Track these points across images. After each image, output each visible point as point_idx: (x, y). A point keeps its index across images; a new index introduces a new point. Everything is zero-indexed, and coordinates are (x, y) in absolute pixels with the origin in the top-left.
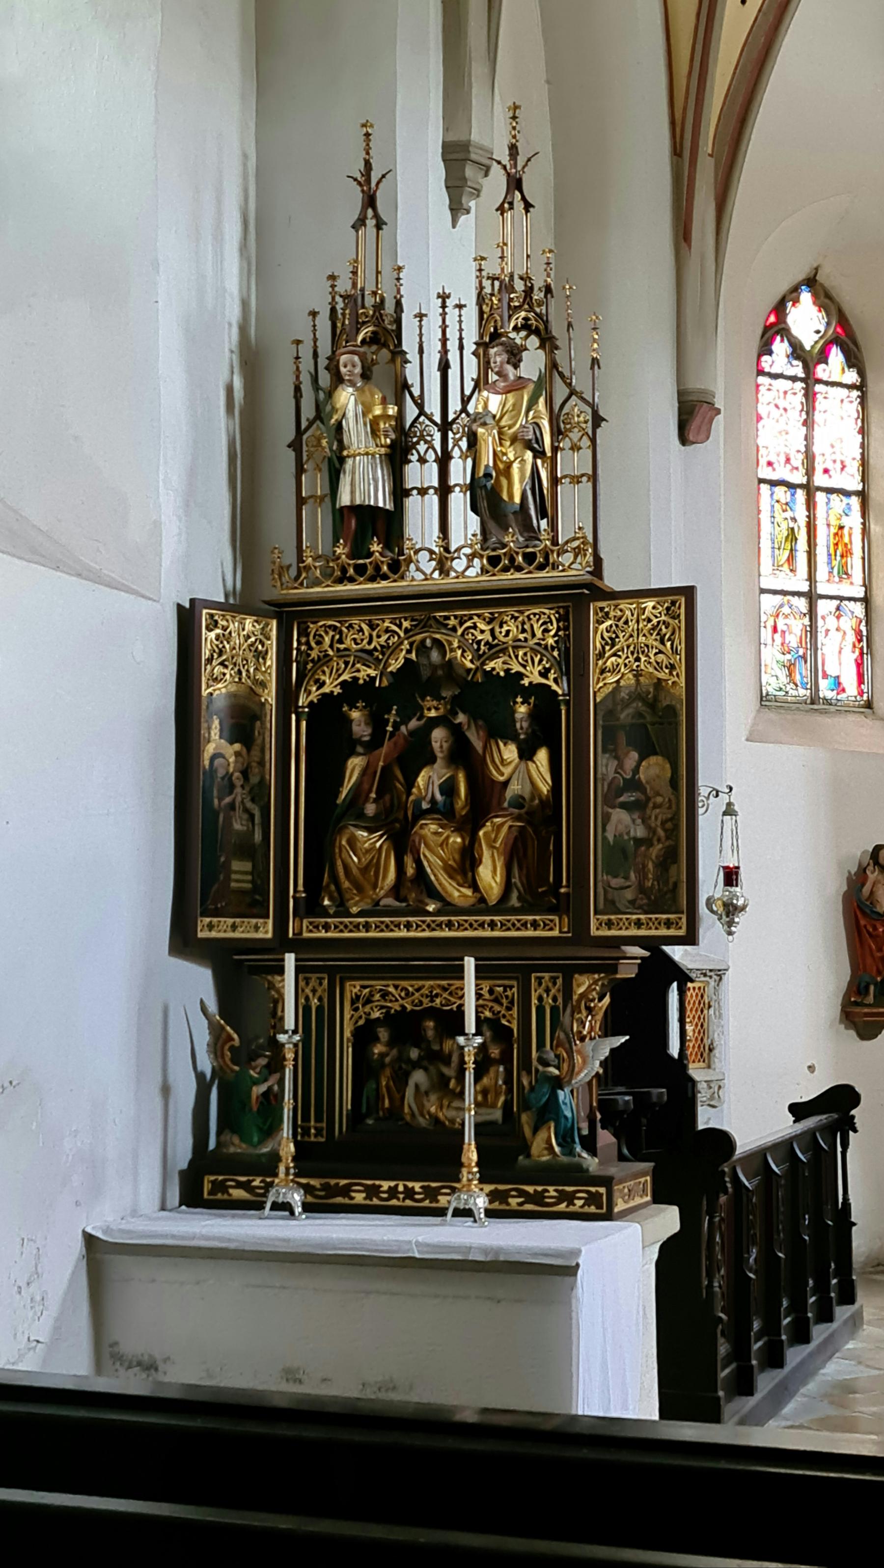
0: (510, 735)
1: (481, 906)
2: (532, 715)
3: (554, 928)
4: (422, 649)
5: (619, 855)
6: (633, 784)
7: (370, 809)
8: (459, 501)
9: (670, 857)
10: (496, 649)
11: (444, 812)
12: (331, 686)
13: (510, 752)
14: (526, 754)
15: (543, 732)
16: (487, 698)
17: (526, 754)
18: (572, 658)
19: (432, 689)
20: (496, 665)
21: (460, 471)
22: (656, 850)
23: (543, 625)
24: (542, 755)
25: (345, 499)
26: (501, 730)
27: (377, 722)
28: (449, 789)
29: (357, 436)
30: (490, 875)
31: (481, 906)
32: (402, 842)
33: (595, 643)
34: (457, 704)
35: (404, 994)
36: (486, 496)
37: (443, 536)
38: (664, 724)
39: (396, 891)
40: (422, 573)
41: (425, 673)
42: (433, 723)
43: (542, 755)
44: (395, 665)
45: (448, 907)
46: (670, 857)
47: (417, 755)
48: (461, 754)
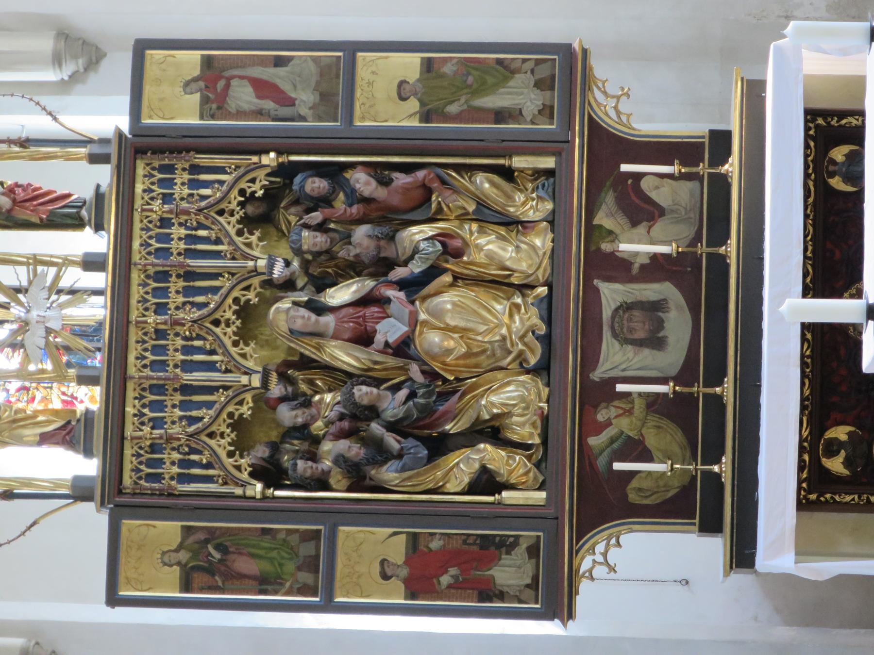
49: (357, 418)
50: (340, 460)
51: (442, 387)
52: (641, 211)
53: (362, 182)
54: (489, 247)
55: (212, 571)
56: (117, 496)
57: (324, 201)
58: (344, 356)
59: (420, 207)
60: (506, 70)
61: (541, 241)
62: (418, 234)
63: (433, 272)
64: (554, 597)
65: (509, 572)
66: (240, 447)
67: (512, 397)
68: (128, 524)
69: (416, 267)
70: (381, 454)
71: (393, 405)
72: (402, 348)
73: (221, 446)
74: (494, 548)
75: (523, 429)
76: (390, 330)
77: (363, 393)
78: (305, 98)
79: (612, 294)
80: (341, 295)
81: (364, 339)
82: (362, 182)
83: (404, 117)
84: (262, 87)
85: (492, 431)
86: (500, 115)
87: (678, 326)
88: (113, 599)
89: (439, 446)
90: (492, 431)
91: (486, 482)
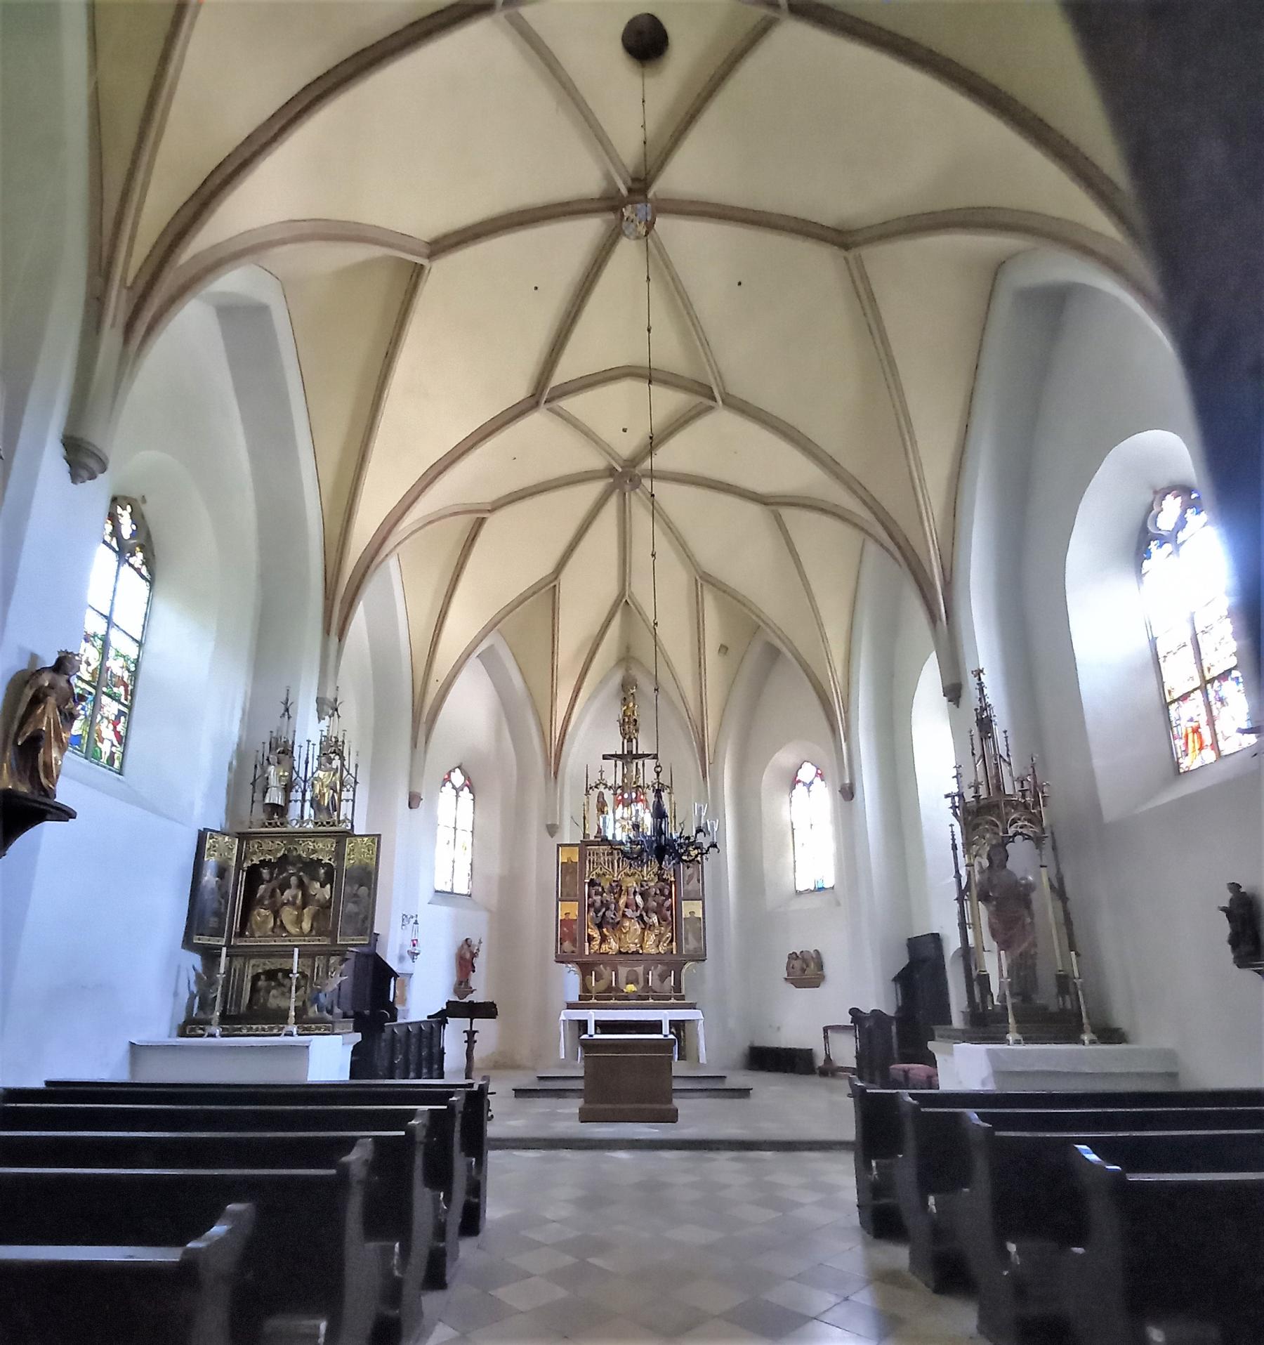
0: (317, 880)
1: (302, 934)
2: (325, 873)
3: (327, 941)
4: (289, 850)
5: (350, 918)
6: (356, 895)
7: (266, 902)
8: (307, 805)
9: (366, 918)
10: (314, 851)
11: (292, 903)
12: (256, 861)
13: (318, 885)
14: (323, 886)
15: (329, 879)
16: (311, 866)
17: (323, 886)
18: (339, 855)
19: (293, 864)
20: (314, 856)
21: (308, 796)
22: (361, 916)
23: (330, 844)
24: (328, 886)
25: (267, 801)
26: (314, 878)
27: (271, 874)
28: (295, 897)
29: (273, 781)
30: (306, 926)
31: (302, 934)
32: (276, 914)
33: (347, 850)
34: (300, 870)
35: (271, 964)
36: (316, 803)
37: (301, 814)
38: (367, 878)
39: (273, 930)
40: (294, 826)
41: (291, 859)
42: (292, 874)
43: (328, 886)
44: (279, 855)
45: (289, 934)
46: (366, 918)
47: (285, 886)
48: (301, 885)
49: (605, 905)
50: (594, 902)
51: (616, 926)
52: (663, 977)
53: (667, 903)
54: (651, 939)
55: (566, 869)
56: (586, 843)
57: (662, 894)
58: (622, 901)
59: (662, 919)
60: (698, 940)
61: (653, 951)
62: (655, 919)
63: (644, 922)
64: (561, 960)
65: (567, 946)
66: (598, 875)
67: (613, 945)
68: (577, 849)
69: (645, 918)
70: (597, 912)
71: (610, 914)
72: (624, 915)
73: (598, 871)
74: (574, 942)
75: (605, 947)
76: (629, 912)
77: (613, 906)
78: (690, 887)
79: (640, 970)
80: (639, 899)
81: (627, 906)
82: (667, 903)
83: (685, 914)
84: (691, 877)
85: (604, 939)
86: (686, 939)
87: (631, 988)
88: (559, 845)
89: (600, 926)
90: (604, 939)
91: (591, 939)
